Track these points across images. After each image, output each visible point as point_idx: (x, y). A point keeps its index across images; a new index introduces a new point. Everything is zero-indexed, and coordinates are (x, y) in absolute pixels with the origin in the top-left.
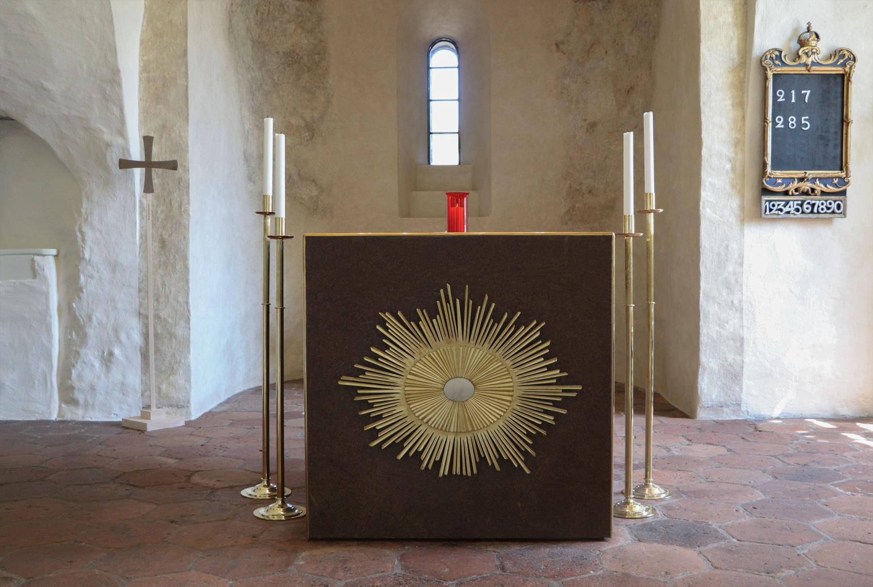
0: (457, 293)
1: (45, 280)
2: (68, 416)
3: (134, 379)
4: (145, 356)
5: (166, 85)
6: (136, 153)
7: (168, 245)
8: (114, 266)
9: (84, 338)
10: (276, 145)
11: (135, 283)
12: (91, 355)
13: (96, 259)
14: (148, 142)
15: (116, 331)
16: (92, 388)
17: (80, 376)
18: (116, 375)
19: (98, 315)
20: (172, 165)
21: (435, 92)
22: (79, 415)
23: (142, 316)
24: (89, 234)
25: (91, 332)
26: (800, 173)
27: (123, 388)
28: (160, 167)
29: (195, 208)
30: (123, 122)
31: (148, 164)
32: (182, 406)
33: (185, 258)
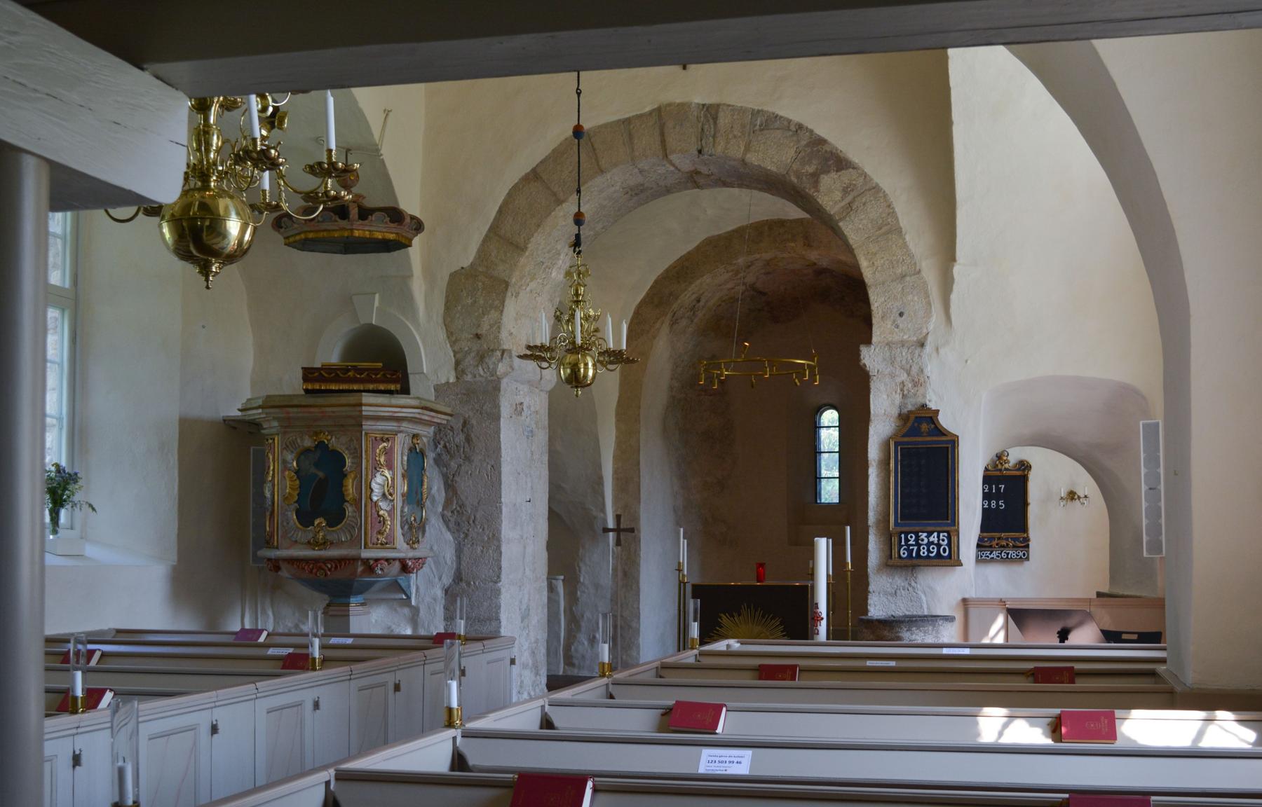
0: (749, 607)
1: (558, 594)
2: (569, 673)
5: (628, 483)
6: (611, 525)
7: (628, 574)
8: (597, 586)
9: (579, 628)
10: (683, 543)
11: (609, 596)
12: (583, 638)
13: (587, 582)
16: (583, 657)
17: (576, 650)
19: (588, 614)
20: (632, 530)
24: (583, 569)
25: (583, 624)
26: (997, 535)
28: (626, 532)
30: (604, 504)
33: (638, 582)
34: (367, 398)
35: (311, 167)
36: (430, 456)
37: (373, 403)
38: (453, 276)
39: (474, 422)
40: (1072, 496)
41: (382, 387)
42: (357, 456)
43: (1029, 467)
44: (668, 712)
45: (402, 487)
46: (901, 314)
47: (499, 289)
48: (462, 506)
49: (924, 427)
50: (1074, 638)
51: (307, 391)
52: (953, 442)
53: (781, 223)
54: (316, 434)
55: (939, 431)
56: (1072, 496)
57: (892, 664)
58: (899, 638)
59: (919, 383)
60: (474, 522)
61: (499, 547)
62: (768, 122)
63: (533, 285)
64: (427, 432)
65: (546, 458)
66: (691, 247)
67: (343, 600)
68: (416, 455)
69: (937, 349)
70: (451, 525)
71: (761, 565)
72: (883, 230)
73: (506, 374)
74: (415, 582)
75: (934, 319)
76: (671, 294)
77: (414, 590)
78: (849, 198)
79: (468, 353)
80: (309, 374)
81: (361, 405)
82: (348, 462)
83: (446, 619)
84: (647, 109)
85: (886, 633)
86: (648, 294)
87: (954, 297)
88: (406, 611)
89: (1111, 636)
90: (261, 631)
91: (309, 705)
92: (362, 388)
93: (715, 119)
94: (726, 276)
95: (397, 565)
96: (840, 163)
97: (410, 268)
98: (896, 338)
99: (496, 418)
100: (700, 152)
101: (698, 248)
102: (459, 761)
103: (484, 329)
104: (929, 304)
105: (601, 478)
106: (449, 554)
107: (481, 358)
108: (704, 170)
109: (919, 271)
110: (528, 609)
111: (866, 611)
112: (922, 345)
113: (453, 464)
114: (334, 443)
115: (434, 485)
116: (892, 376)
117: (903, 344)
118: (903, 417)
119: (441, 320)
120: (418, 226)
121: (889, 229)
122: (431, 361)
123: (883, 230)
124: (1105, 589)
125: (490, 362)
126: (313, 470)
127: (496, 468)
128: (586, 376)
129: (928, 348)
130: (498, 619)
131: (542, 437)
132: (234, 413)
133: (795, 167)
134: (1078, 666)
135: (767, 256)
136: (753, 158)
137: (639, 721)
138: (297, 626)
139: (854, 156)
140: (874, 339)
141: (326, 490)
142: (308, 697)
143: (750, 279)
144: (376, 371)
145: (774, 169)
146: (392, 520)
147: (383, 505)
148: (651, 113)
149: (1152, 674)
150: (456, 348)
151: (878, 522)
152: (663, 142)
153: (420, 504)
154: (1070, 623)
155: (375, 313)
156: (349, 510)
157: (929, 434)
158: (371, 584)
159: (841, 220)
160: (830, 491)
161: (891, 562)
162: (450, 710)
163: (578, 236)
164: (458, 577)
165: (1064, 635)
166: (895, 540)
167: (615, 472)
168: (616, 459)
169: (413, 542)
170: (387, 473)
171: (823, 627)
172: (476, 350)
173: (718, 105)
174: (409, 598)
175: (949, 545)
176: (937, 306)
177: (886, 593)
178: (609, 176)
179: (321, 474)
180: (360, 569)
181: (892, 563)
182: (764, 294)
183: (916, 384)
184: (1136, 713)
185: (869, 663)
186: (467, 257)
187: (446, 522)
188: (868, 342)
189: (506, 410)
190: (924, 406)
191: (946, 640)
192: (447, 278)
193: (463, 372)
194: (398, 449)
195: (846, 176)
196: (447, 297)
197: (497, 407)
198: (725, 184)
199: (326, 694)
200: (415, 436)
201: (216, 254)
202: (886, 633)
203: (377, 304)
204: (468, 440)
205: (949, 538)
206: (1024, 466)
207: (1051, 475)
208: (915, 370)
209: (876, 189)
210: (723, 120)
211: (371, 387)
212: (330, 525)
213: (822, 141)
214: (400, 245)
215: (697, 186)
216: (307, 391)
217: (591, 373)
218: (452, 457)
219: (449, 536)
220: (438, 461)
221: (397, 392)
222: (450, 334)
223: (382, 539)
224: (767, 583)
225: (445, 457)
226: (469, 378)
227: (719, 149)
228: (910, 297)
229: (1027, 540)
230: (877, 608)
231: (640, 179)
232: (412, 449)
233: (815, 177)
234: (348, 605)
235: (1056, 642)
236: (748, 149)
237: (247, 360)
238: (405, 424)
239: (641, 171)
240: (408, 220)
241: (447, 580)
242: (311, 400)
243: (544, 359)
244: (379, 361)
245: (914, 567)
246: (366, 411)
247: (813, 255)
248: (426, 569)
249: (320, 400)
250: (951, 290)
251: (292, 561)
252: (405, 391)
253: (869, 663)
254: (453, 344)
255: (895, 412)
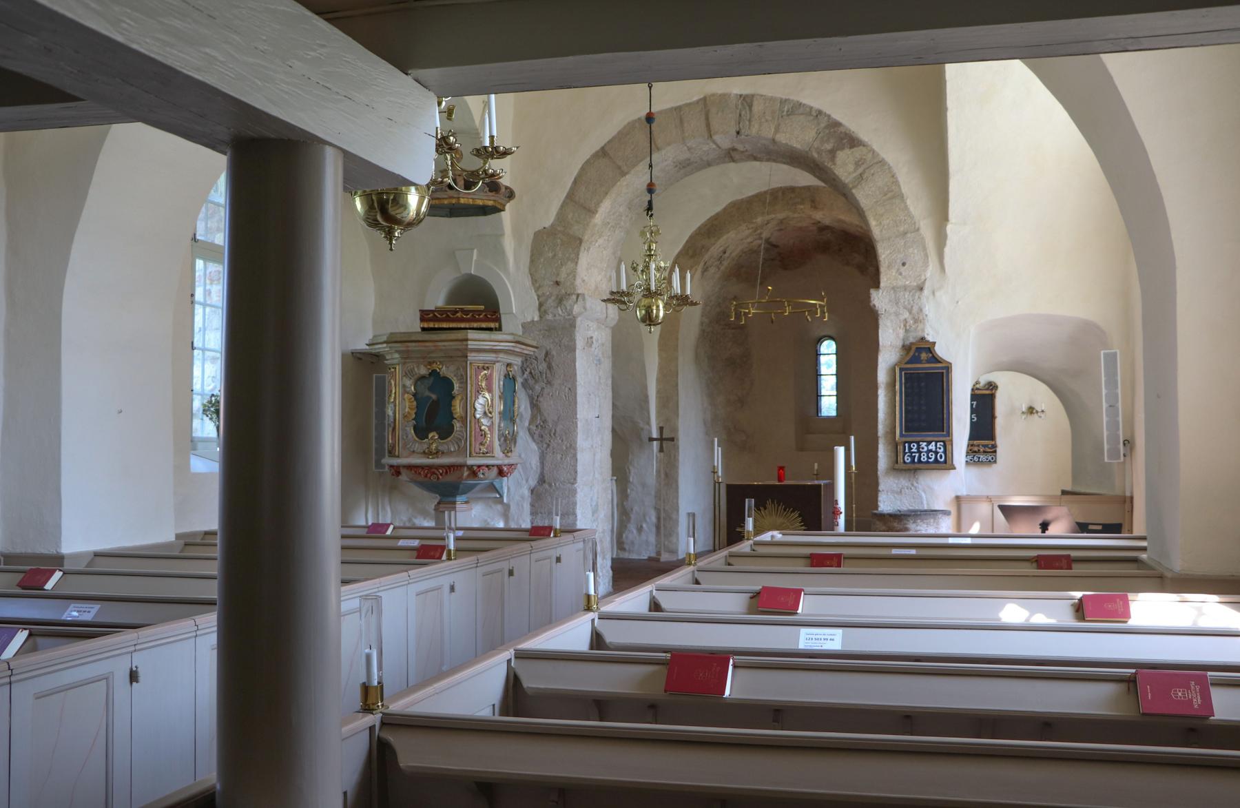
3: (652, 538)
4: (658, 528)
5: (668, 401)
6: (655, 435)
8: (644, 485)
9: (629, 519)
10: (718, 452)
12: (632, 527)
14: (661, 429)
15: (644, 516)
16: (633, 543)
18: (644, 537)
19: (636, 508)
21: (824, 370)
22: (626, 555)
23: (658, 510)
24: (633, 471)
25: (633, 516)
27: (647, 542)
28: (667, 440)
29: (681, 458)
30: (649, 418)
31: (661, 439)
32: (674, 552)
33: (677, 481)
34: (472, 335)
35: (478, 150)
36: (519, 380)
37: (476, 339)
38: (538, 235)
39: (554, 353)
40: (1031, 410)
41: (484, 325)
42: (464, 382)
43: (996, 387)
44: (756, 595)
45: (499, 407)
46: (904, 264)
47: (576, 243)
48: (545, 421)
49: (924, 356)
50: (1052, 530)
51: (423, 329)
52: (948, 368)
53: (792, 189)
54: (430, 364)
55: (935, 359)
56: (1031, 410)
57: (913, 552)
58: (907, 529)
59: (918, 318)
60: (554, 435)
61: (575, 456)
62: (796, 109)
63: (600, 241)
64: (517, 361)
65: (610, 382)
66: (719, 209)
67: (451, 499)
68: (510, 379)
69: (933, 293)
70: (536, 437)
71: (781, 468)
72: (890, 195)
73: (580, 314)
74: (506, 484)
75: (930, 268)
76: (703, 247)
77: (505, 491)
78: (860, 170)
79: (549, 297)
80: (425, 315)
81: (467, 340)
82: (456, 386)
83: (532, 514)
84: (695, 99)
85: (895, 524)
86: (684, 246)
87: (947, 250)
88: (499, 507)
89: (1082, 528)
90: (388, 525)
91: (447, 589)
92: (467, 325)
93: (750, 106)
94: (747, 232)
95: (495, 471)
96: (852, 141)
97: (502, 229)
98: (900, 283)
99: (572, 349)
100: (738, 133)
101: (725, 209)
102: (597, 640)
103: (562, 278)
104: (926, 256)
105: (646, 397)
106: (534, 461)
107: (560, 301)
108: (740, 147)
109: (918, 230)
110: (597, 505)
111: (877, 507)
112: (921, 289)
113: (538, 388)
114: (444, 371)
115: (523, 405)
116: (897, 314)
117: (905, 288)
118: (906, 348)
119: (527, 270)
120: (511, 195)
121: (893, 195)
122: (519, 303)
123: (890, 195)
124: (1069, 488)
125: (568, 303)
126: (427, 393)
127: (573, 390)
128: (657, 316)
129: (926, 292)
130: (575, 514)
131: (607, 365)
132: (362, 346)
133: (816, 144)
134: (1074, 554)
135: (781, 216)
136: (782, 138)
137: (733, 604)
138: (410, 520)
139: (863, 135)
140: (882, 285)
141: (438, 411)
142: (445, 582)
143: (764, 236)
144: (480, 312)
145: (799, 146)
146: (492, 434)
147: (484, 421)
148: (698, 102)
149: (1135, 560)
150: (540, 293)
151: (886, 433)
152: (708, 125)
153: (513, 421)
154: (1048, 516)
155: (474, 265)
156: (457, 425)
157: (928, 361)
158: (475, 485)
159: (854, 187)
160: (829, 405)
161: (897, 466)
162: (589, 596)
163: (650, 202)
164: (542, 480)
165: (1044, 526)
166: (900, 448)
167: (658, 392)
168: (658, 380)
169: (507, 451)
170: (487, 395)
171: (842, 520)
172: (557, 295)
173: (753, 96)
174: (501, 496)
175: (945, 452)
176: (933, 258)
177: (893, 492)
178: (663, 152)
179: (434, 397)
180: (466, 474)
181: (897, 468)
182: (775, 246)
183: (916, 321)
184: (1142, 596)
185: (895, 552)
186: (548, 220)
187: (532, 435)
188: (877, 285)
189: (580, 343)
190: (923, 339)
191: (944, 531)
192: (532, 236)
193: (545, 312)
194: (496, 376)
195: (858, 152)
196: (532, 251)
197: (573, 340)
198: (756, 159)
199: (459, 579)
200: (509, 365)
201: (398, 222)
202: (895, 524)
203: (475, 257)
204: (550, 367)
205: (945, 446)
206: (992, 386)
207: (1014, 393)
208: (915, 309)
209: (882, 162)
210: (757, 107)
211: (475, 325)
212: (441, 438)
213: (837, 124)
214: (496, 210)
215: (733, 160)
216: (423, 329)
217: (661, 314)
218: (536, 382)
219: (534, 446)
220: (525, 385)
221: (496, 329)
222: (534, 281)
223: (484, 449)
224: (786, 482)
225: (531, 382)
226: (550, 317)
227: (754, 131)
228: (911, 250)
229: (994, 446)
230: (886, 504)
231: (687, 155)
232: (507, 376)
233: (832, 153)
234: (454, 503)
235: (1039, 532)
236: (777, 130)
237: (370, 303)
238: (501, 355)
239: (689, 149)
240: (503, 190)
241: (533, 482)
242: (427, 336)
243: (624, 303)
244: (476, 305)
245: (916, 470)
246: (471, 344)
247: (818, 216)
248: (516, 473)
249: (434, 336)
250: (945, 245)
251: (410, 467)
252: (500, 329)
253: (895, 552)
254: (537, 290)
255: (900, 344)
